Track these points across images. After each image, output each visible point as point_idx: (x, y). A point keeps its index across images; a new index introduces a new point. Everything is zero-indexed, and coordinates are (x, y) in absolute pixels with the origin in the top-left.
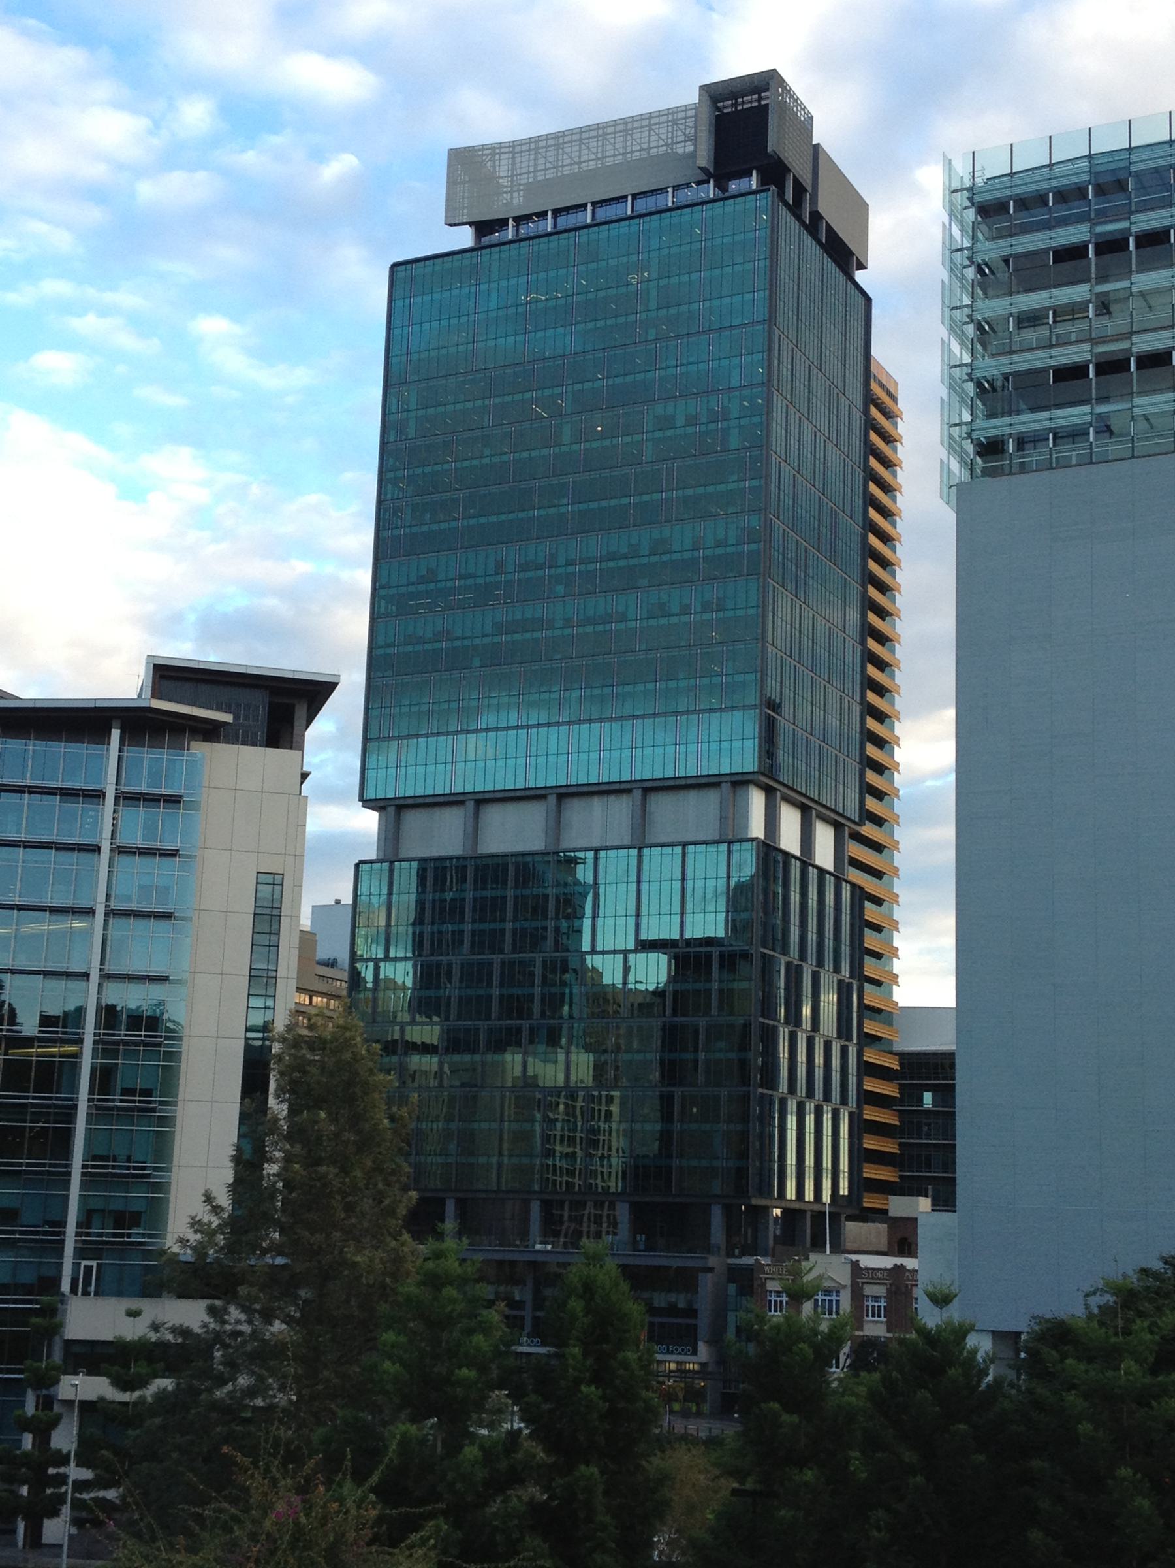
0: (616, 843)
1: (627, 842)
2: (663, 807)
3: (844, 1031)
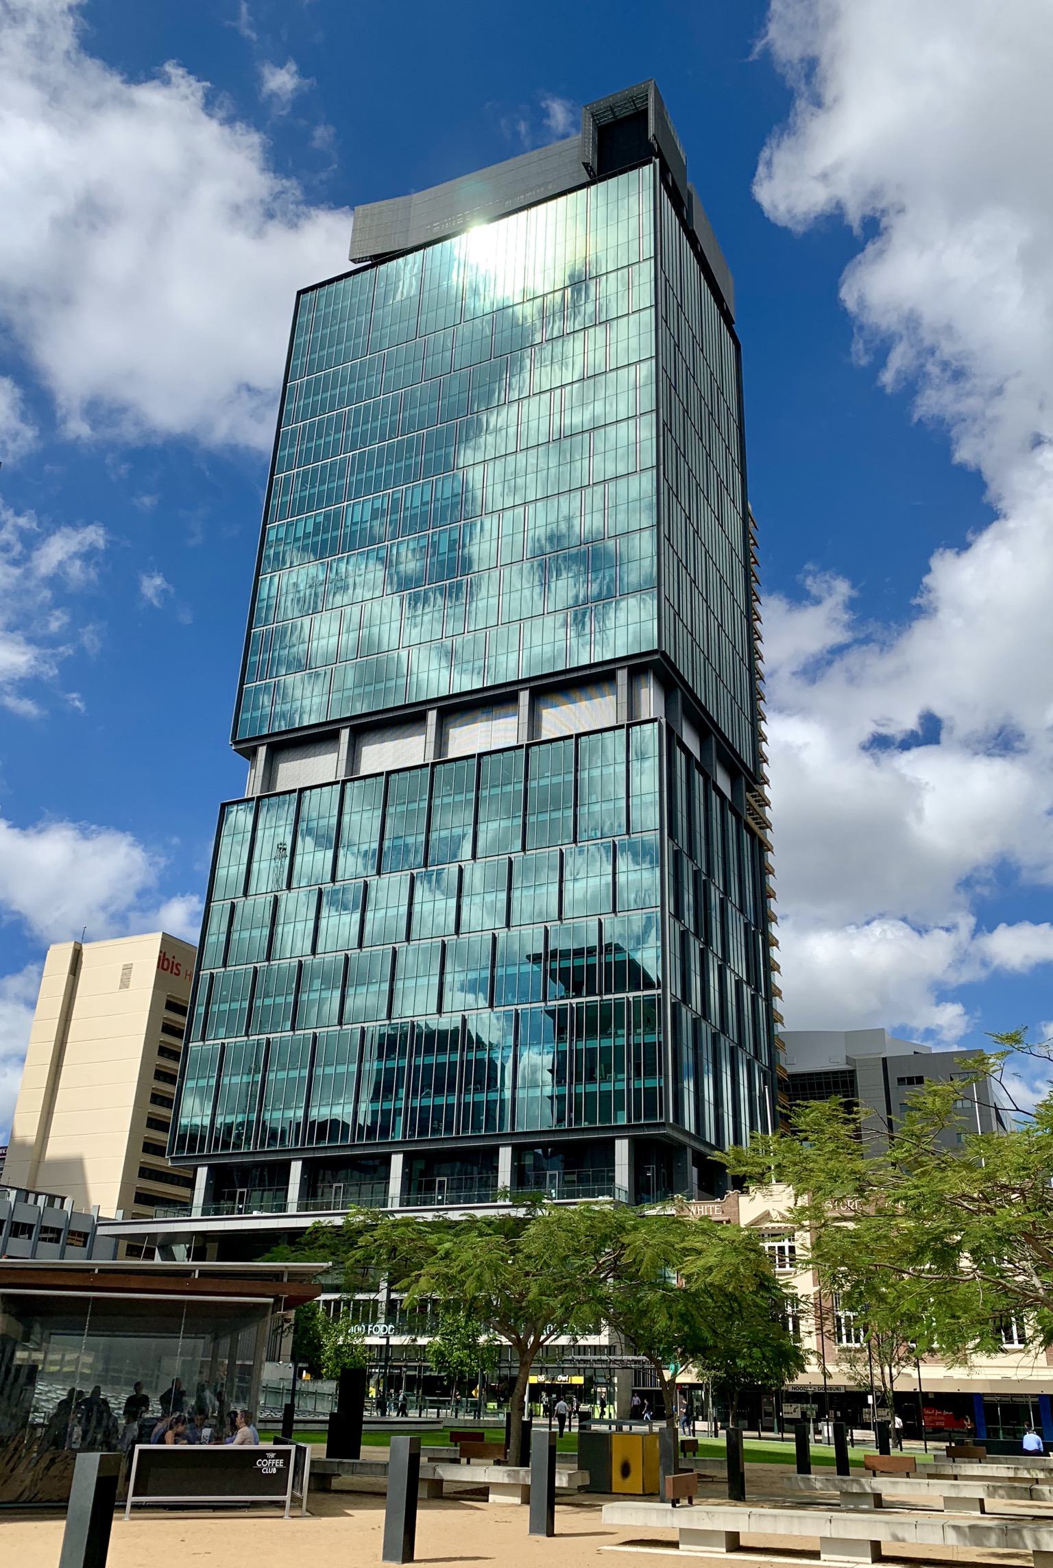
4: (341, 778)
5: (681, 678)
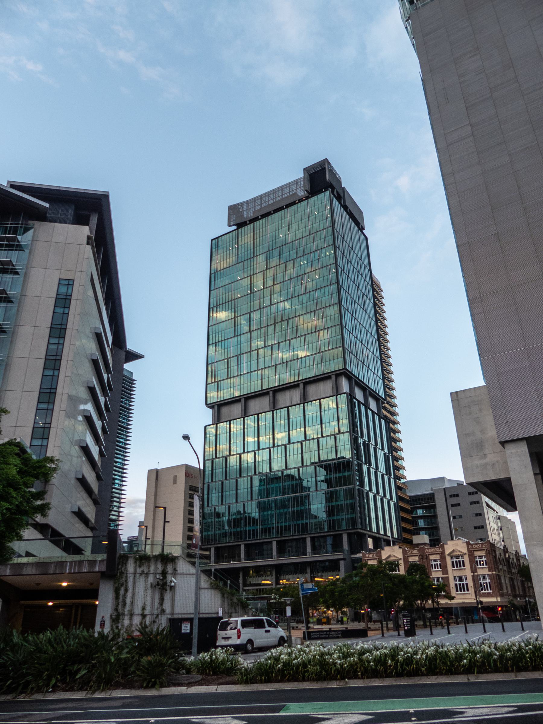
0: (295, 404)
1: (299, 402)
3: (388, 472)
5: (354, 375)
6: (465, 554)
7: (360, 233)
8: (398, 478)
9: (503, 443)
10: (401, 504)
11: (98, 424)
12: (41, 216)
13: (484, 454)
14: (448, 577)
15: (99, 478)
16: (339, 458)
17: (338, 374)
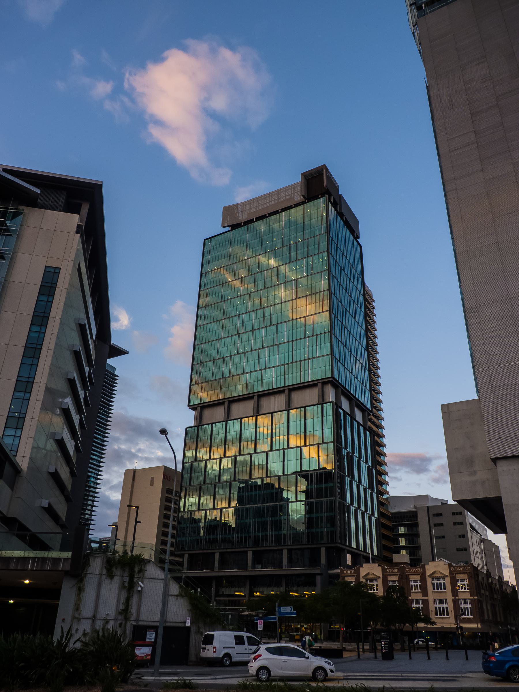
1: (284, 409)
2: (297, 397)
3: (371, 486)
4: (226, 420)
5: (341, 384)
6: (447, 576)
7: (355, 241)
8: (381, 493)
9: (495, 460)
10: (383, 520)
11: (76, 418)
12: (33, 202)
13: (474, 471)
14: (427, 600)
15: (72, 474)
16: (322, 469)
17: (325, 382)
